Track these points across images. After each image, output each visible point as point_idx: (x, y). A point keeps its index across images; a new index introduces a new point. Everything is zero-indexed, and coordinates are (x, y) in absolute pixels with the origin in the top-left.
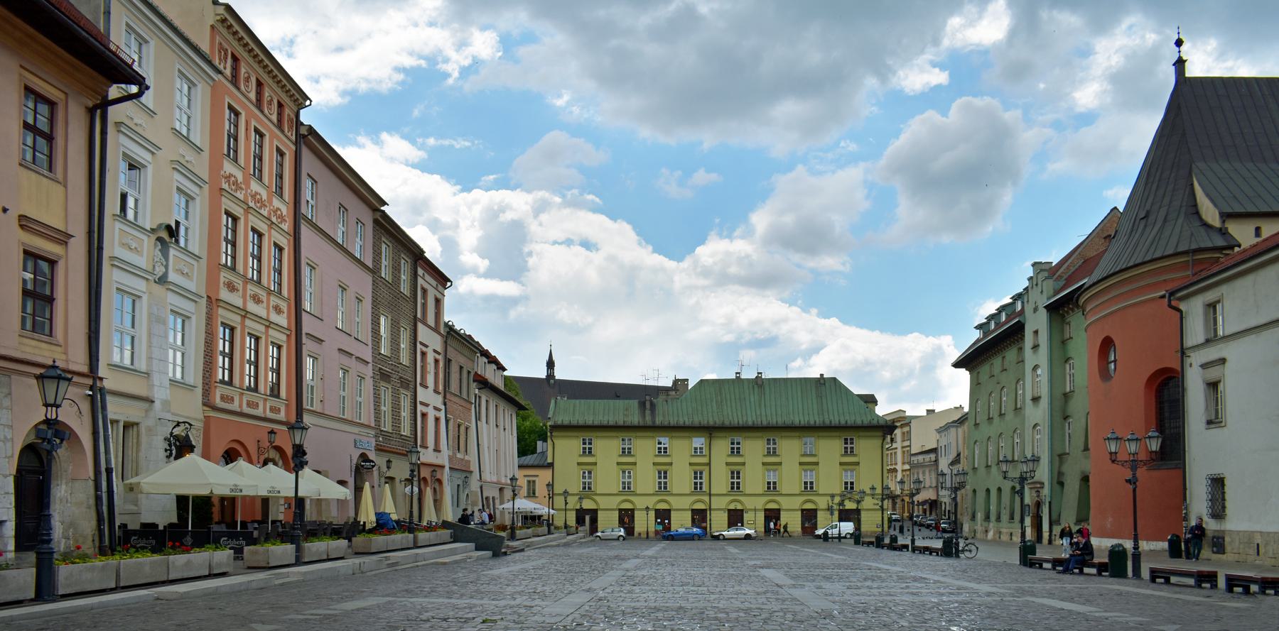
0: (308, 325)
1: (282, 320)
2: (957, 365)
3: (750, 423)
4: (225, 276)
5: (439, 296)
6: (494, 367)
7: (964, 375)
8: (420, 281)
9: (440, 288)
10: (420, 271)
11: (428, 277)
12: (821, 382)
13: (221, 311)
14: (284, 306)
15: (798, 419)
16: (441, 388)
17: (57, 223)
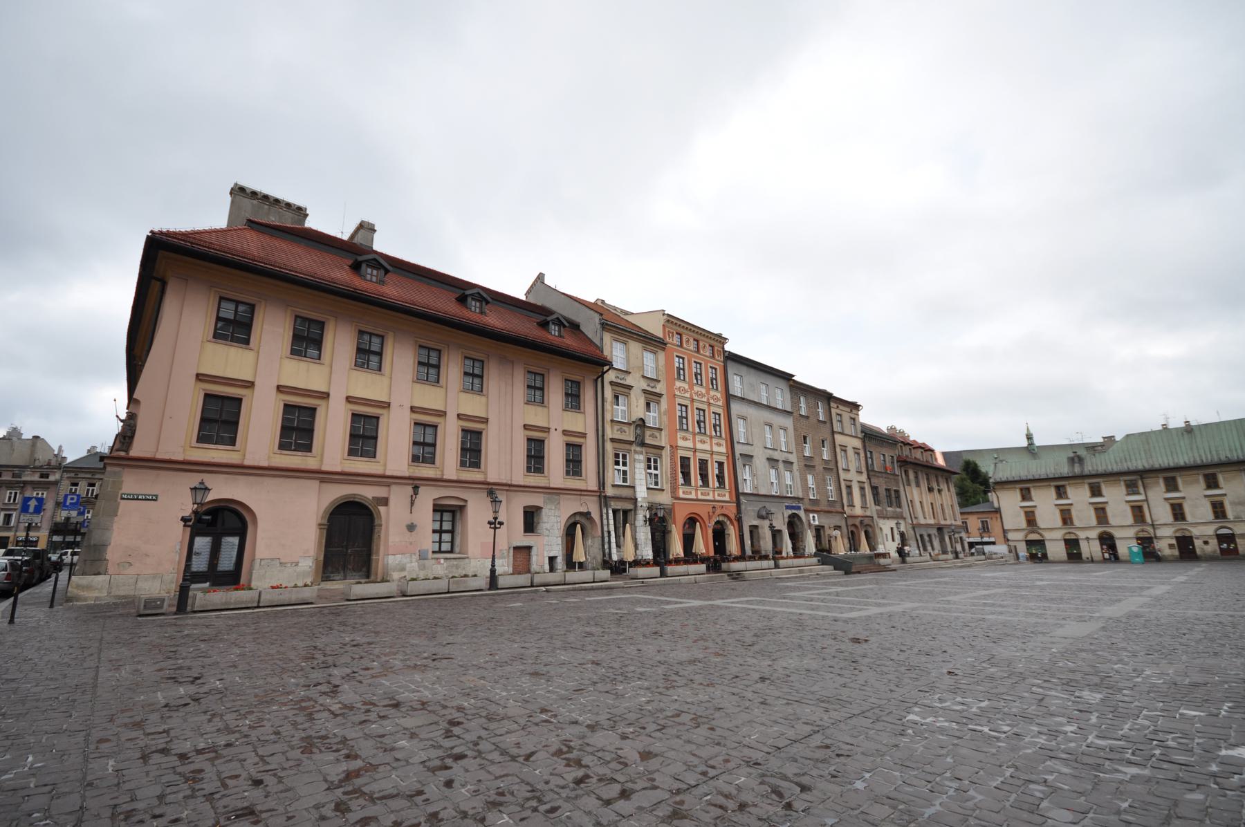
0: (739, 449)
1: (723, 449)
4: (680, 434)
8: (834, 411)
10: (833, 405)
14: (723, 442)
16: (864, 469)
17: (580, 430)
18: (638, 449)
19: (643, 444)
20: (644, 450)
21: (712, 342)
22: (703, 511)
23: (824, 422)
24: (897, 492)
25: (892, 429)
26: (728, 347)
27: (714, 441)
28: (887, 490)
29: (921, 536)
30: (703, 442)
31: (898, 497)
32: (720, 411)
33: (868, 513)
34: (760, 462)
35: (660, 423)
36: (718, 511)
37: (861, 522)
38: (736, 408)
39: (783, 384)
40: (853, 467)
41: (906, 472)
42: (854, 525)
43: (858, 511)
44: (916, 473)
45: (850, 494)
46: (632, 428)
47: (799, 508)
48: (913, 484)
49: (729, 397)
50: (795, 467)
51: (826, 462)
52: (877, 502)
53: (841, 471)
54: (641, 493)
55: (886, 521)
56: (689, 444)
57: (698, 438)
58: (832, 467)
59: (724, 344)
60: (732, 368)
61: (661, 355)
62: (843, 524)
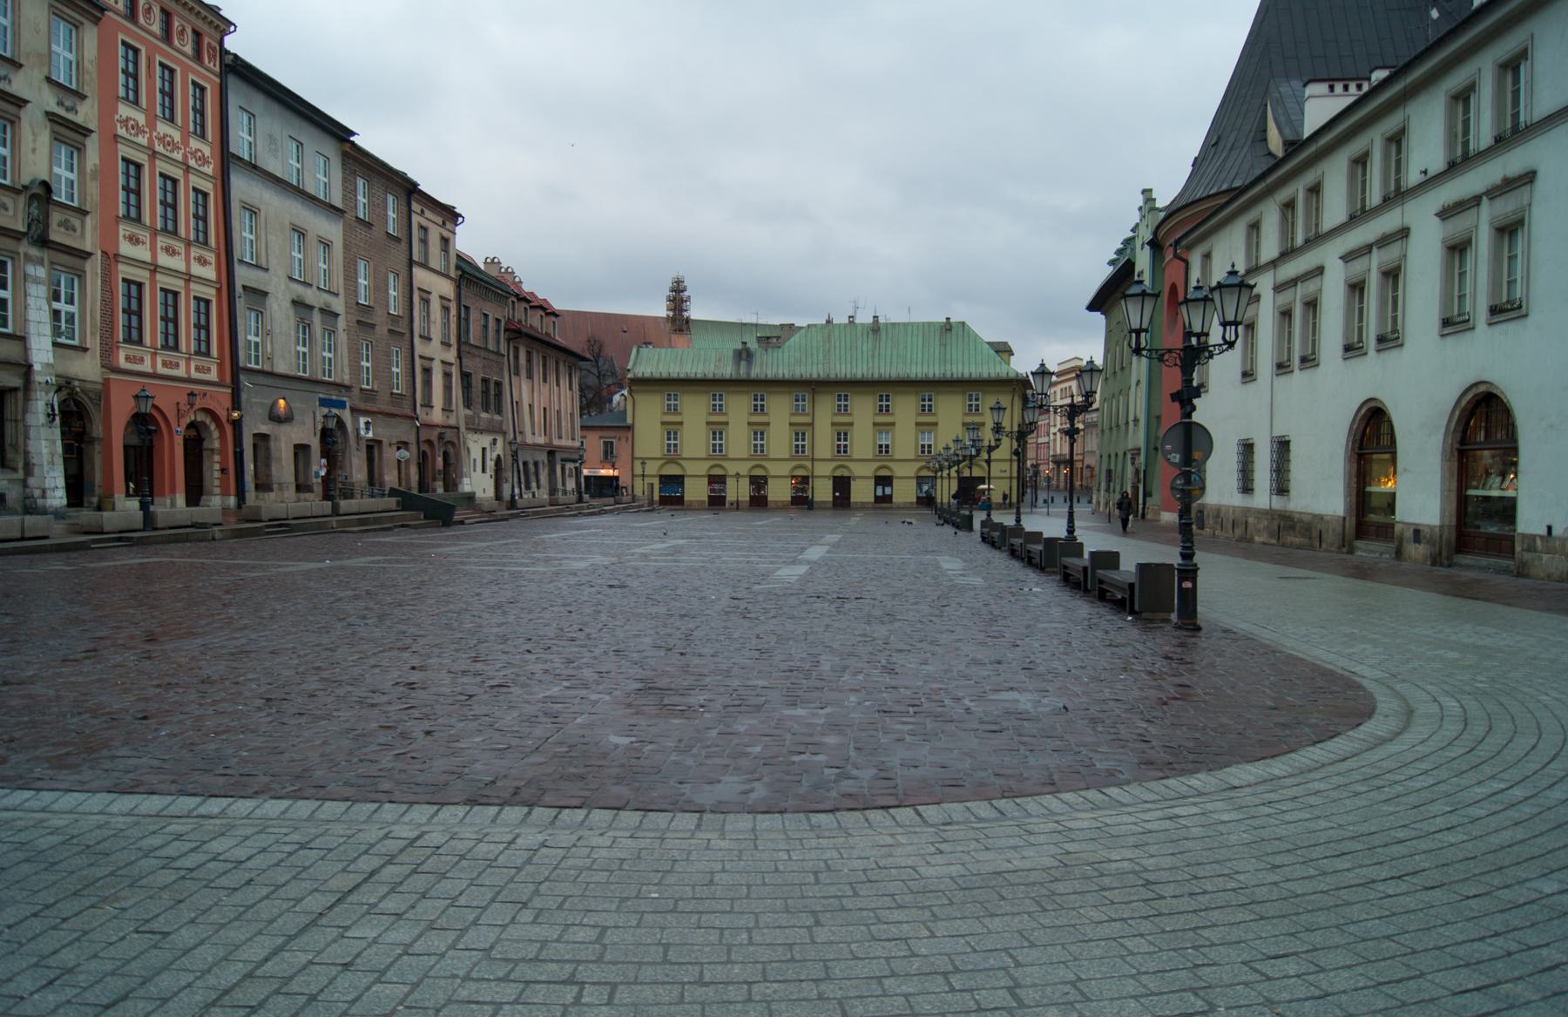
0: (243, 276)
1: (210, 273)
2: (1092, 307)
3: (859, 376)
4: (124, 229)
5: (446, 234)
6: (541, 312)
7: (1098, 318)
8: (415, 219)
9: (449, 225)
10: (416, 207)
11: (428, 213)
12: (948, 327)
13: (121, 267)
14: (211, 257)
15: (916, 371)
16: (453, 340)
18: (34, 252)
19: (43, 242)
20: (46, 255)
21: (200, 25)
22: (166, 400)
23: (397, 240)
24: (498, 385)
25: (493, 262)
26: (231, 43)
27: (195, 252)
28: (485, 381)
29: (525, 464)
30: (170, 251)
31: (499, 395)
32: (207, 186)
33: (452, 422)
34: (279, 309)
35: (83, 199)
36: (199, 403)
37: (441, 437)
38: (242, 187)
39: (330, 148)
40: (436, 332)
41: (516, 349)
42: (429, 442)
43: (437, 416)
44: (529, 353)
45: (428, 383)
46: (22, 200)
47: (342, 405)
48: (523, 373)
49: (227, 160)
50: (341, 323)
51: (395, 319)
52: (468, 403)
53: (417, 340)
54: (41, 352)
55: (476, 437)
56: (142, 253)
57: (161, 241)
58: (403, 332)
59: (224, 33)
60: (238, 95)
61: (90, 35)
62: (412, 439)
